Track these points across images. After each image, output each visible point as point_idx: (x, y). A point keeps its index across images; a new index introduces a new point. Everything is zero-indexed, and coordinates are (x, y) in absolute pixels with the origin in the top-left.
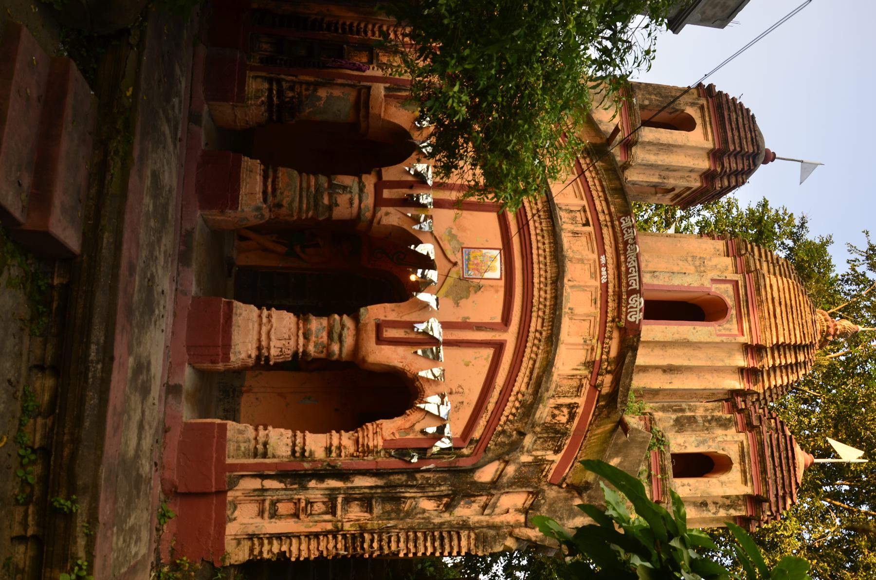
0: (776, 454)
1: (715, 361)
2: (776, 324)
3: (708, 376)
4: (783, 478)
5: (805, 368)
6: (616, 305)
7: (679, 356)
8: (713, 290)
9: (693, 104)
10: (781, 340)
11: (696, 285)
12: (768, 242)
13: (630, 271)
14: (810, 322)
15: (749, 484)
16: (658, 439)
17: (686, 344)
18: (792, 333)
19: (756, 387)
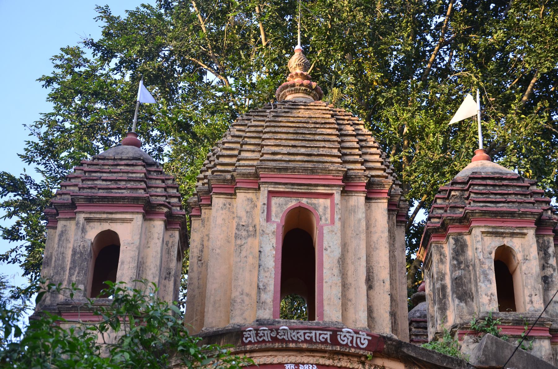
0: (492, 198)
1: (361, 229)
2: (318, 155)
3: (375, 238)
4: (516, 194)
5: (358, 124)
6: (345, 358)
7: (356, 270)
8: (278, 220)
9: (84, 230)
10: (335, 152)
11: (274, 241)
12: (107, 87)
15: (525, 231)
16: (488, 325)
17: (342, 261)
18: (327, 137)
19: (386, 186)
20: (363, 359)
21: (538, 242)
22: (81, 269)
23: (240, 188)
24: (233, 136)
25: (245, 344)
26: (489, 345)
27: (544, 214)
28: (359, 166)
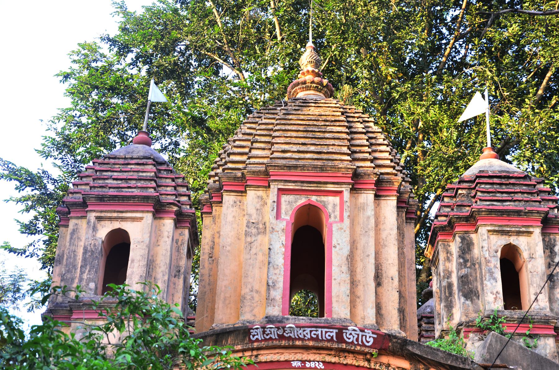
0: (499, 196)
1: (369, 227)
3: (384, 235)
5: (368, 122)
6: (351, 355)
7: (364, 267)
9: (95, 229)
10: (345, 149)
11: (283, 238)
12: (123, 82)
13: (315, 336)
14: (319, 109)
15: (531, 230)
16: (493, 323)
17: (351, 258)
19: (395, 184)
20: (368, 356)
21: (543, 240)
22: (92, 267)
23: (250, 186)
24: (243, 134)
25: (252, 342)
26: (494, 343)
27: (551, 212)
28: (368, 164)
